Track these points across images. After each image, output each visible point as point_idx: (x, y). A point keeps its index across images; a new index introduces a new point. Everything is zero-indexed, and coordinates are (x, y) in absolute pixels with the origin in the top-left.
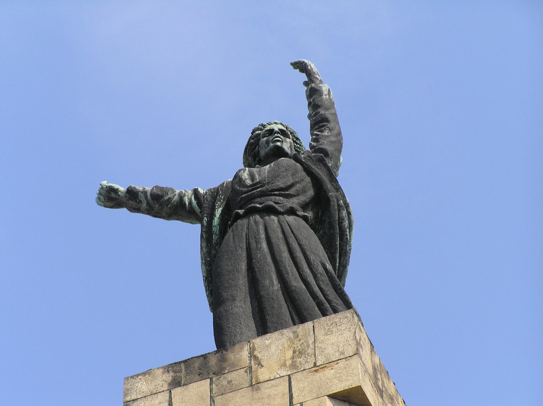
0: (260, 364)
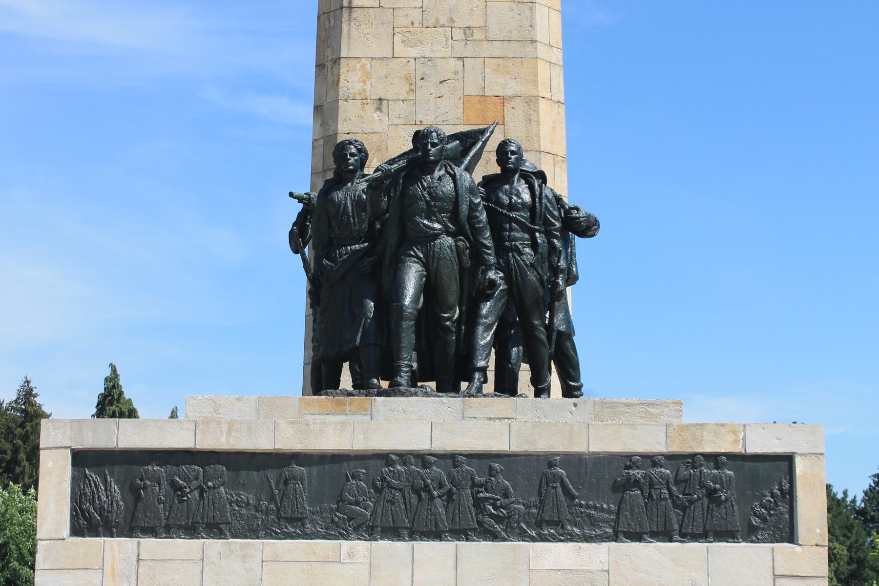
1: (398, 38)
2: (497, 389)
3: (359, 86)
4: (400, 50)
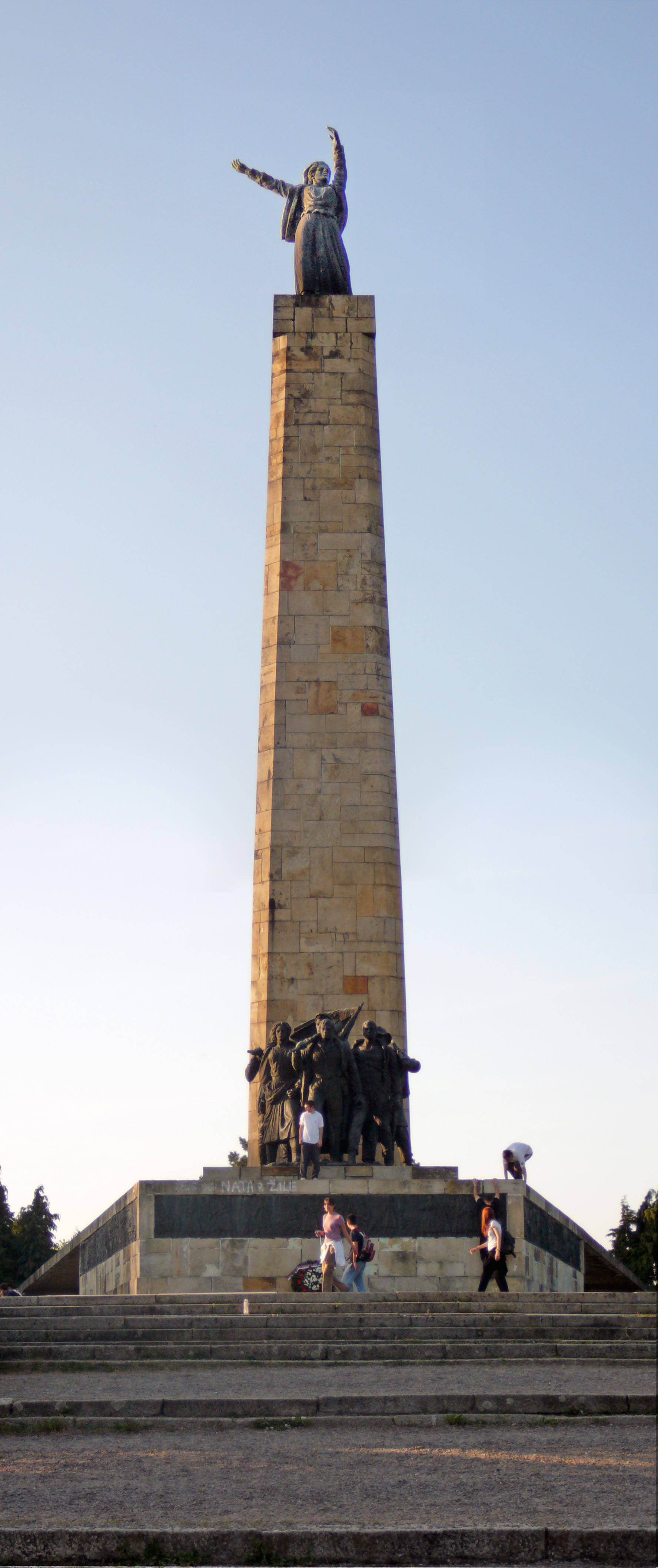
0: (333, 308)
1: (303, 940)
2: (363, 1160)
3: (279, 970)
4: (304, 947)
